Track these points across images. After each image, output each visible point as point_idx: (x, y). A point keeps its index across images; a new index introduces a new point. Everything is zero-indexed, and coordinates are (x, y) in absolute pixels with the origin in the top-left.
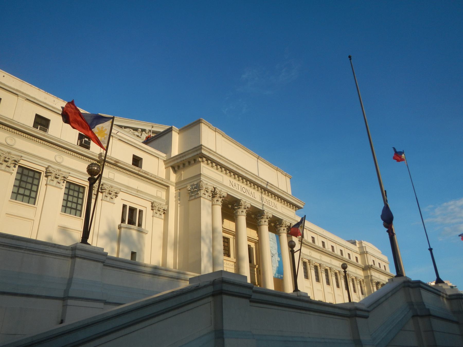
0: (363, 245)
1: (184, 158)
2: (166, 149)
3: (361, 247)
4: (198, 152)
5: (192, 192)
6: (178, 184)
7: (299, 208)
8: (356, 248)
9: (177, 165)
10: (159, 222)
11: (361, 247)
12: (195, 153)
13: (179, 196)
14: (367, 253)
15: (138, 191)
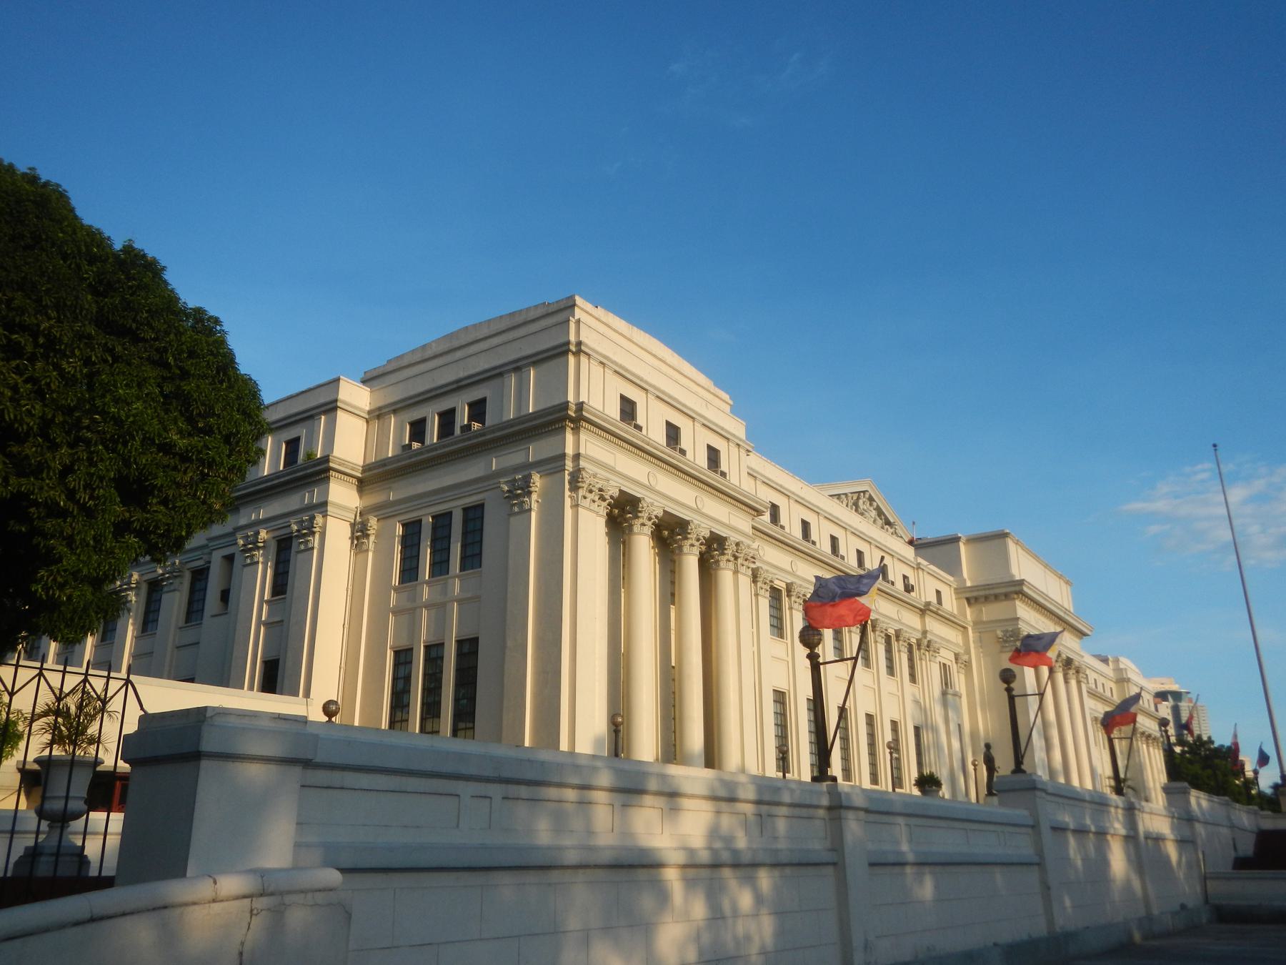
0: (1122, 666)
1: (992, 592)
2: (952, 566)
3: (1118, 670)
4: (1017, 588)
5: (1005, 641)
6: (977, 623)
7: (1085, 634)
8: (1108, 670)
9: (975, 597)
10: (962, 677)
11: (1118, 670)
12: (1013, 589)
13: (980, 642)
14: (1128, 680)
15: (948, 641)
